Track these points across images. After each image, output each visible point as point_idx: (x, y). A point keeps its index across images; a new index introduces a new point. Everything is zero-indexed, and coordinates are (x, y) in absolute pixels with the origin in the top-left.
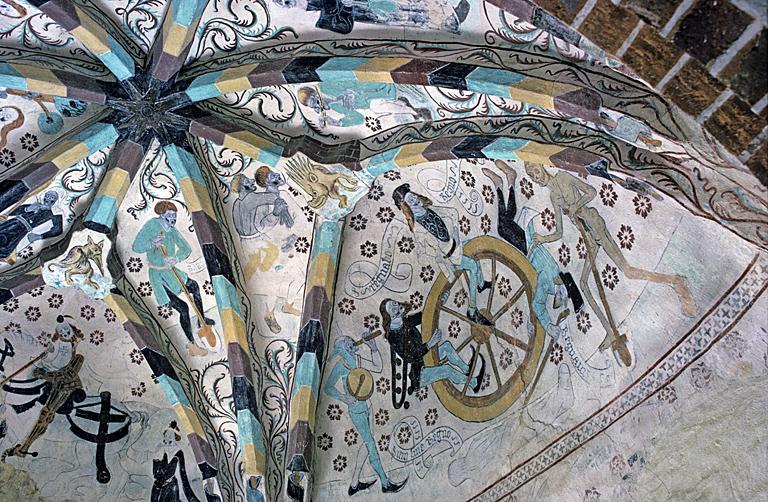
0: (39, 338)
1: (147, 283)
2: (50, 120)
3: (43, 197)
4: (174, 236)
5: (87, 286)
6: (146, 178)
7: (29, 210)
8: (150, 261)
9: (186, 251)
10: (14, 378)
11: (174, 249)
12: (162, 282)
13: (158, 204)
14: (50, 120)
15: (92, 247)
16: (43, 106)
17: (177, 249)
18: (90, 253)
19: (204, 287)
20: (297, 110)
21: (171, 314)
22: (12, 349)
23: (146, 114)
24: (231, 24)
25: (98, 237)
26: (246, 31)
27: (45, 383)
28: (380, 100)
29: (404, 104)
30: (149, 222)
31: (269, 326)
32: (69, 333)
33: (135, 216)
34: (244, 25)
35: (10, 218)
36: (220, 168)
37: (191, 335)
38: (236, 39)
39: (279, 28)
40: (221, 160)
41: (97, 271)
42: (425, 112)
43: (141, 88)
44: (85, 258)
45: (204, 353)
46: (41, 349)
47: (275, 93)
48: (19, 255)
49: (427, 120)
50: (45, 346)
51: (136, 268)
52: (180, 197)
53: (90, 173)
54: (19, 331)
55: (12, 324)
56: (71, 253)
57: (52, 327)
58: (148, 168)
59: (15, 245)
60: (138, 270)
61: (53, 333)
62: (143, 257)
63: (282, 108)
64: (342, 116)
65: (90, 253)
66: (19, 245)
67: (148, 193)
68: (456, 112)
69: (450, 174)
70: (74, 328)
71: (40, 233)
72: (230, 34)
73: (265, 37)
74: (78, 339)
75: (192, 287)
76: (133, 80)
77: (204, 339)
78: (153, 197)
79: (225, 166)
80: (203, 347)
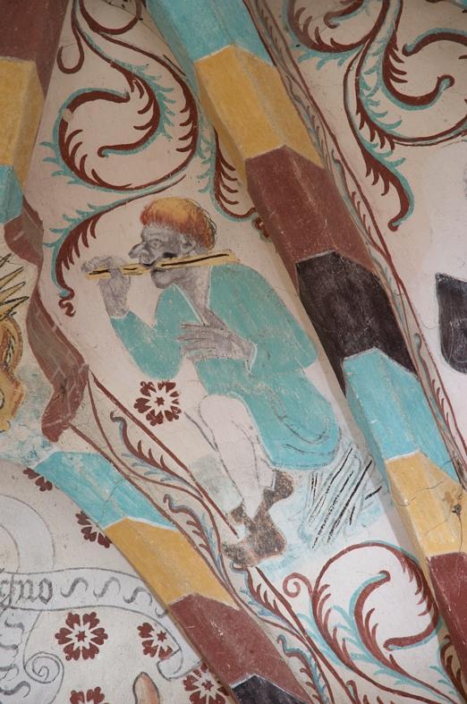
20: (122, 196)
24: (384, 34)
26: (372, 79)
28: (250, 421)
29: (268, 481)
34: (389, 74)
38: (337, 48)
39: (401, 171)
42: (270, 542)
47: (159, 137)
49: (247, 547)
63: (112, 155)
64: (146, 316)
68: (322, 628)
69: (61, 582)
73: (365, 132)
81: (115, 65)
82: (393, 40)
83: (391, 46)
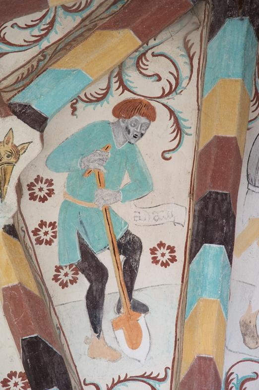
1: (53, 225)
4: (130, 159)
8: (71, 189)
9: (142, 185)
11: (120, 179)
13: (127, 102)
17: (126, 179)
19: (153, 251)
21: (74, 281)
30: (94, 125)
31: (244, 335)
45: (115, 356)
51: (42, 194)
52: (174, 102)
53: (48, 20)
60: (43, 200)
62: (60, 180)
67: (122, 83)
75: (129, 247)
77: (120, 334)
78: (125, 88)
80: (114, 345)
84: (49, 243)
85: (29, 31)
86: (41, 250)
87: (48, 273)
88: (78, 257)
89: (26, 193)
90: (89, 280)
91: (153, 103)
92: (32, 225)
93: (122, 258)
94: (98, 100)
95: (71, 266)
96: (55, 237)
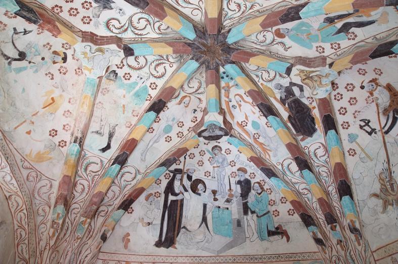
0: (367, 103)
1: (332, 44)
2: (237, 85)
3: (278, 90)
5: (329, 78)
6: (262, 44)
7: (284, 97)
8: (317, 41)
10: (383, 126)
12: (330, 36)
13: (278, 37)
14: (237, 85)
15: (302, 75)
16: (233, 86)
18: (305, 75)
21: (353, 33)
22: (366, 120)
23: (214, 53)
24: (152, 26)
25: (295, 71)
26: (150, 19)
27: (393, 112)
30: (292, 40)
32: (372, 85)
33: (289, 48)
35: (287, 106)
36: (242, 10)
37: (369, 21)
40: (237, 10)
41: (318, 73)
43: (200, 58)
44: (308, 78)
46: (374, 104)
48: (311, 103)
50: (373, 102)
54: (359, 112)
55: (354, 114)
56: (306, 84)
57: (365, 93)
58: (256, 43)
59: (304, 104)
61: (368, 94)
62: (315, 45)
65: (305, 75)
66: (306, 103)
67: (272, 42)
70: (371, 81)
71: (300, 93)
72: (157, 25)
74: (377, 82)
76: (197, 60)
79: (240, 7)
81: (193, 4)
82: (150, 24)
83: (150, 24)
84: (339, 44)
85: (270, 72)
86: (342, 46)
87: (352, 42)
88: (342, 34)
89: (322, 54)
90: (351, 28)
91: (273, 31)
92: (333, 51)
93: (336, 21)
94: (282, 43)
95: (347, 35)
96: (336, 43)
